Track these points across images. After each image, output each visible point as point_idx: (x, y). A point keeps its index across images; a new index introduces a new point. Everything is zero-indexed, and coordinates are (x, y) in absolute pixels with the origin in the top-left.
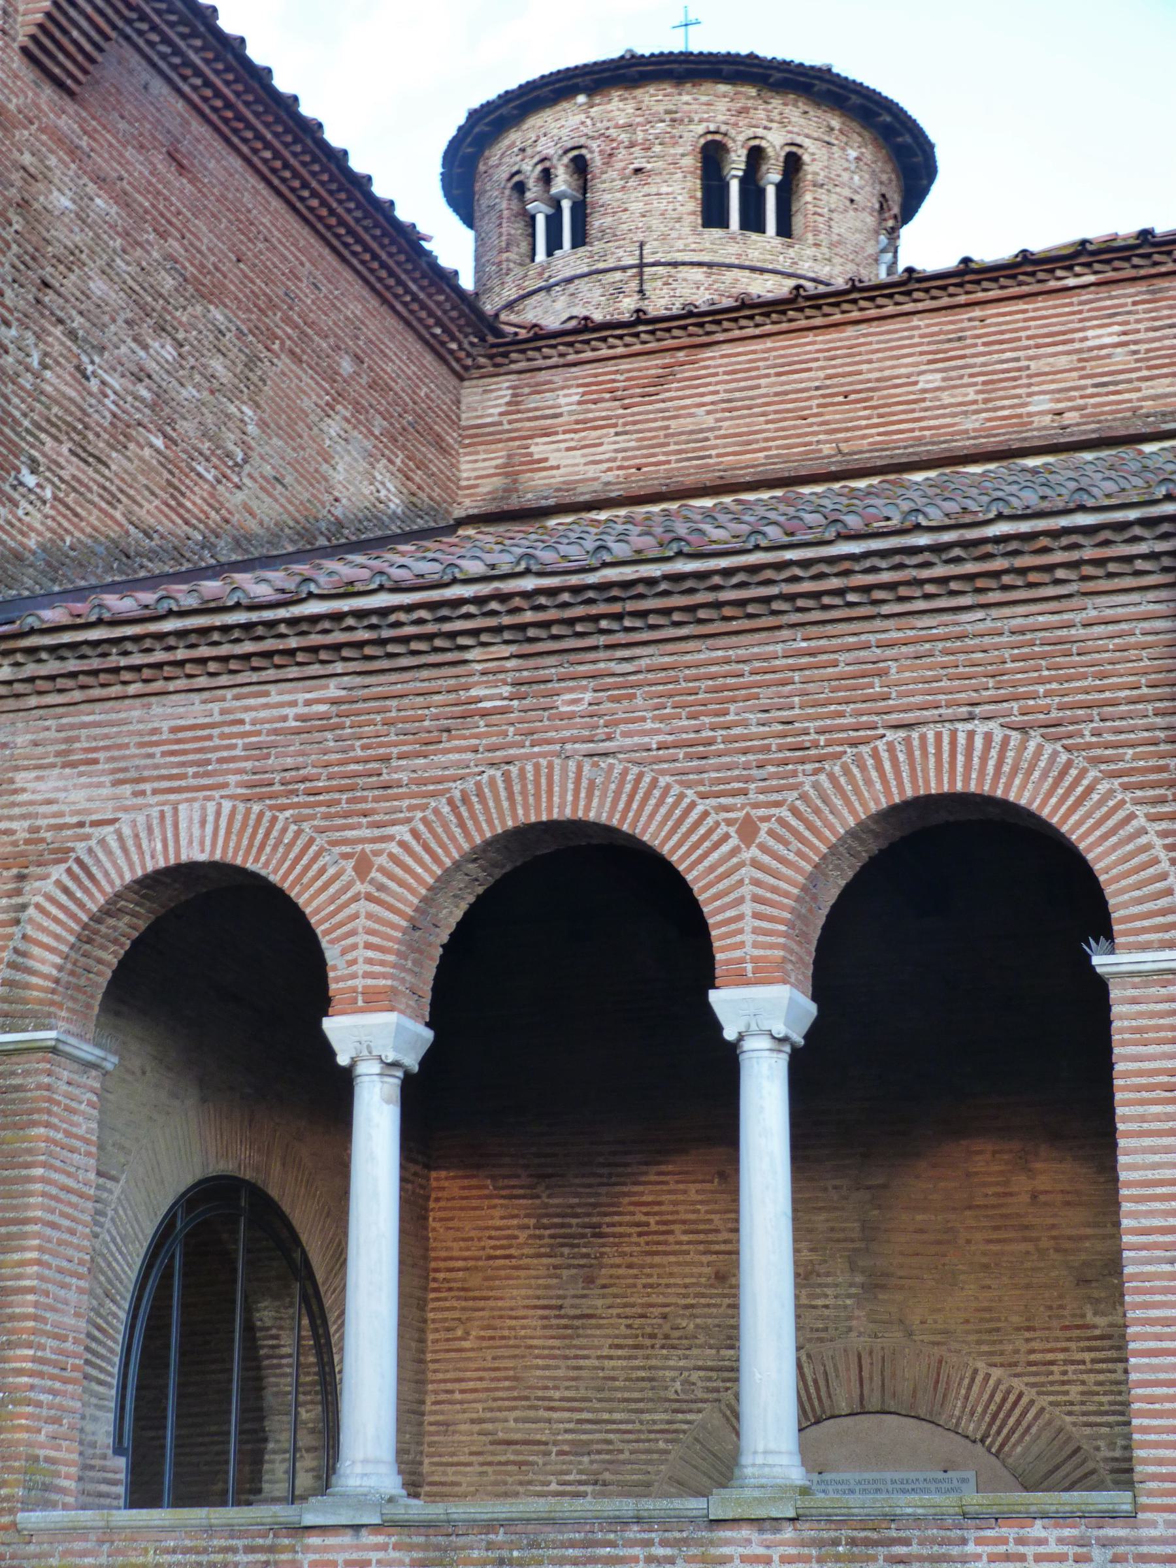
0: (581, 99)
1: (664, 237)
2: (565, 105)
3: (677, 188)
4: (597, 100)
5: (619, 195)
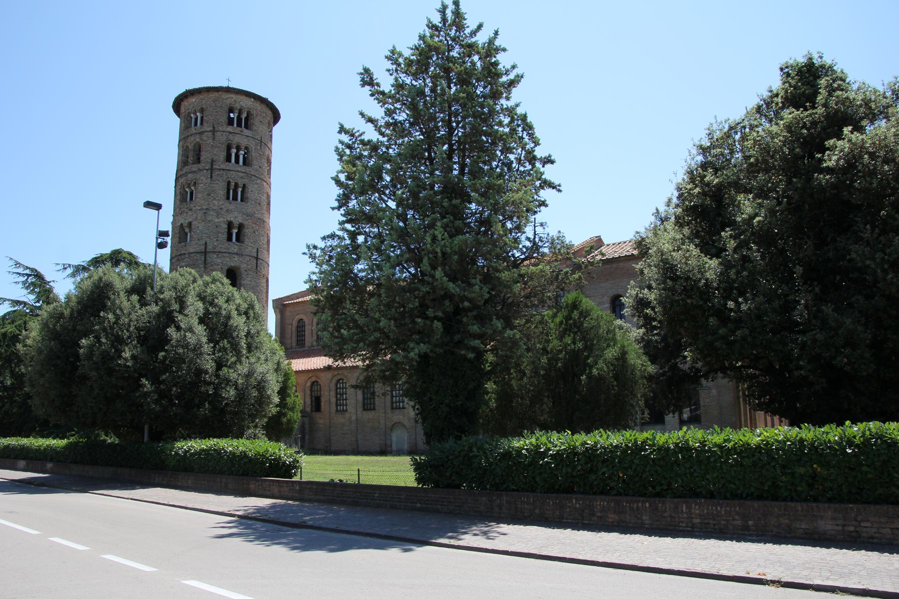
0: (253, 100)
2: (248, 98)
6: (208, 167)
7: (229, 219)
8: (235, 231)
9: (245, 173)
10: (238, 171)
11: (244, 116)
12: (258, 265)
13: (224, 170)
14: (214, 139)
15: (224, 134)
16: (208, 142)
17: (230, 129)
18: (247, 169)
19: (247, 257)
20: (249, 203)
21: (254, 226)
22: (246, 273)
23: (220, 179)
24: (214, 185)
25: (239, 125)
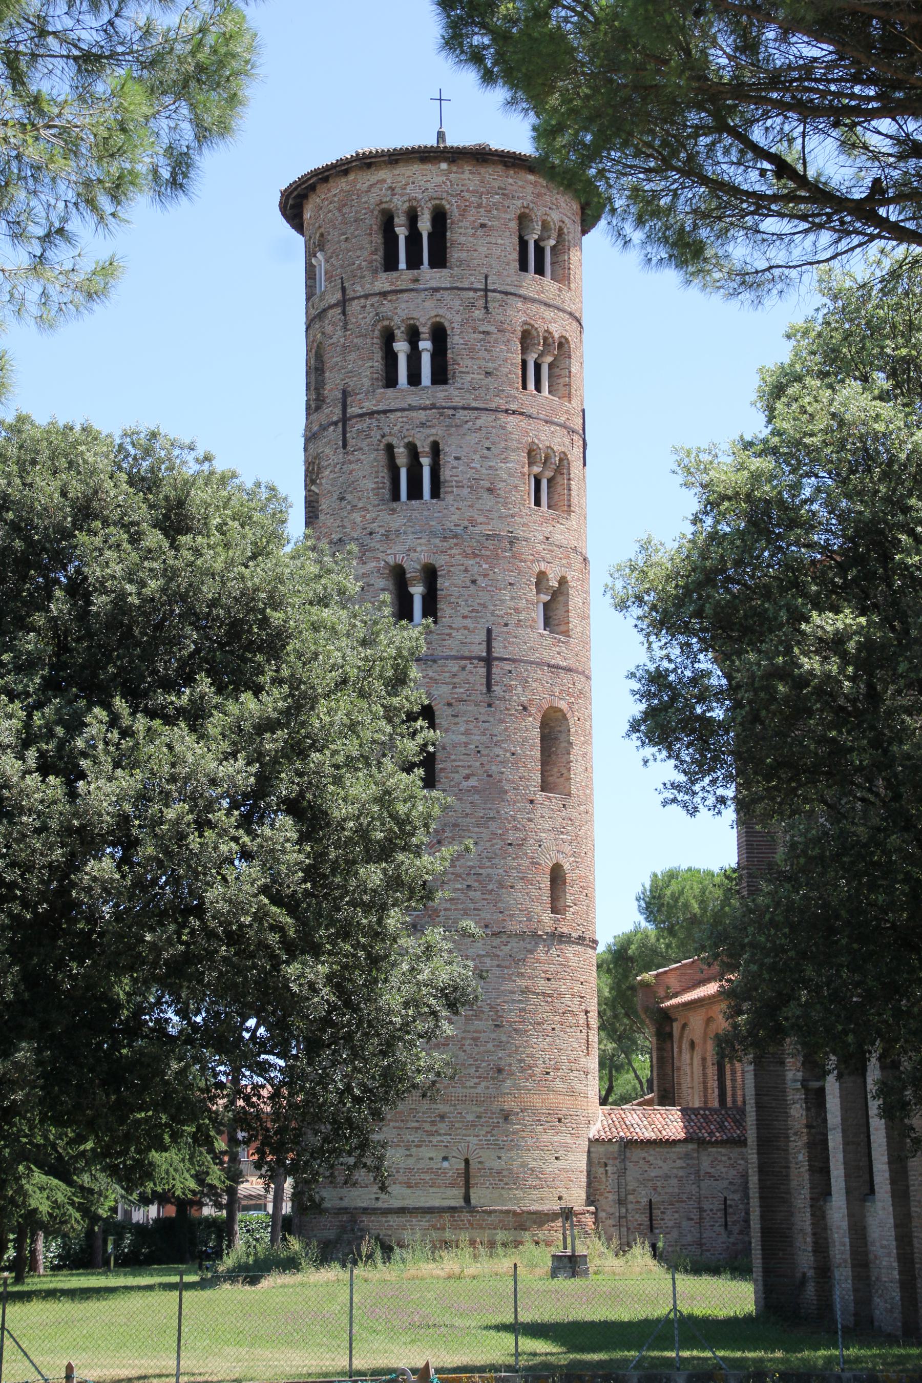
0: (444, 166)
1: (499, 274)
2: (429, 166)
3: (507, 242)
4: (454, 169)
5: (471, 239)
6: (337, 415)
7: (391, 560)
8: (417, 591)
9: (433, 406)
10: (411, 408)
11: (425, 225)
12: (495, 678)
13: (371, 414)
14: (345, 329)
15: (369, 302)
16: (334, 340)
17: (383, 282)
18: (441, 394)
19: (450, 663)
20: (449, 499)
21: (471, 562)
22: (449, 711)
23: (364, 444)
24: (352, 466)
25: (414, 262)
